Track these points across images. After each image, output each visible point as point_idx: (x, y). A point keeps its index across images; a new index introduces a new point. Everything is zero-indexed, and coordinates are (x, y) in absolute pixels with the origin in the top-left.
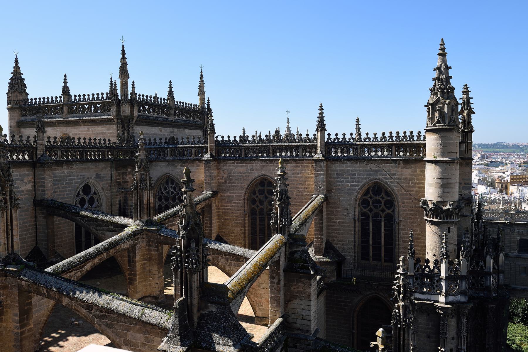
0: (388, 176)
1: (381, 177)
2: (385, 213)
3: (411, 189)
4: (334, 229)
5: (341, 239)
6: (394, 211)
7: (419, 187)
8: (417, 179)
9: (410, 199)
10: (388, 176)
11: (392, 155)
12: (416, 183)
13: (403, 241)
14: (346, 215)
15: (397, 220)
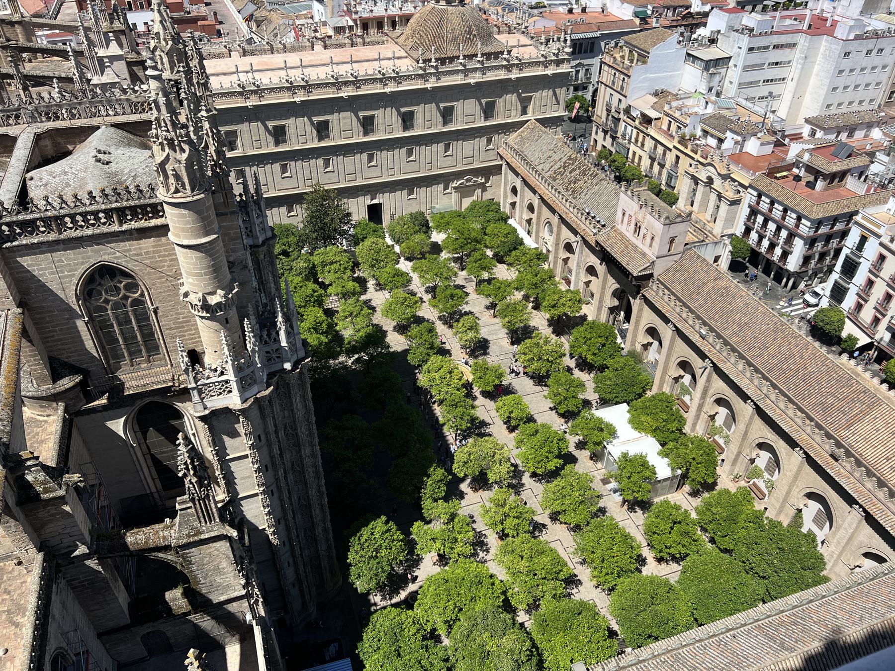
0: (118, 254)
1: (106, 258)
2: (130, 300)
3: (161, 265)
4: (55, 341)
5: (73, 349)
6: (142, 295)
7: (171, 260)
8: (165, 250)
9: (163, 277)
10: (118, 254)
11: (114, 222)
12: (165, 256)
13: (167, 329)
14: (68, 319)
15: (151, 307)
